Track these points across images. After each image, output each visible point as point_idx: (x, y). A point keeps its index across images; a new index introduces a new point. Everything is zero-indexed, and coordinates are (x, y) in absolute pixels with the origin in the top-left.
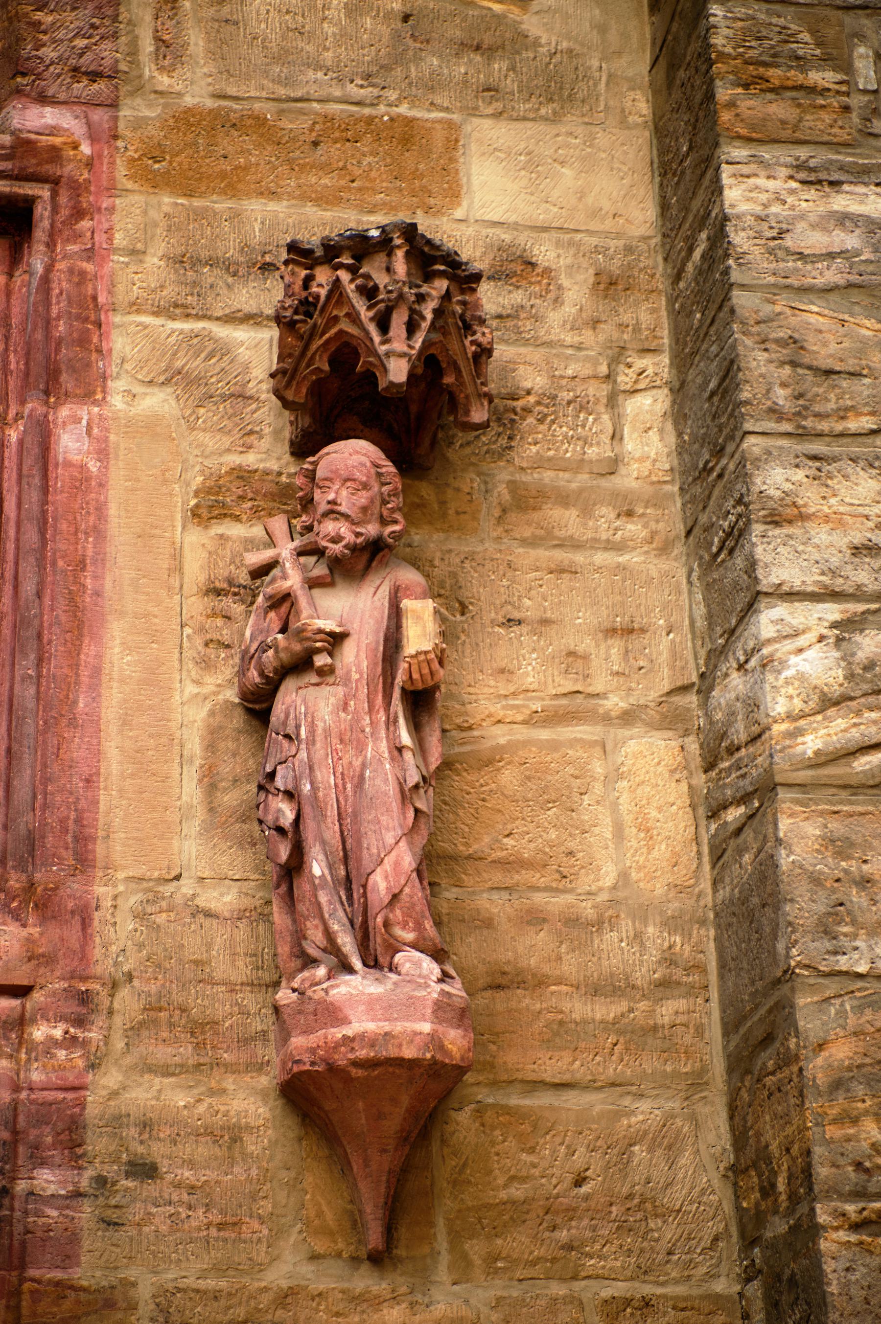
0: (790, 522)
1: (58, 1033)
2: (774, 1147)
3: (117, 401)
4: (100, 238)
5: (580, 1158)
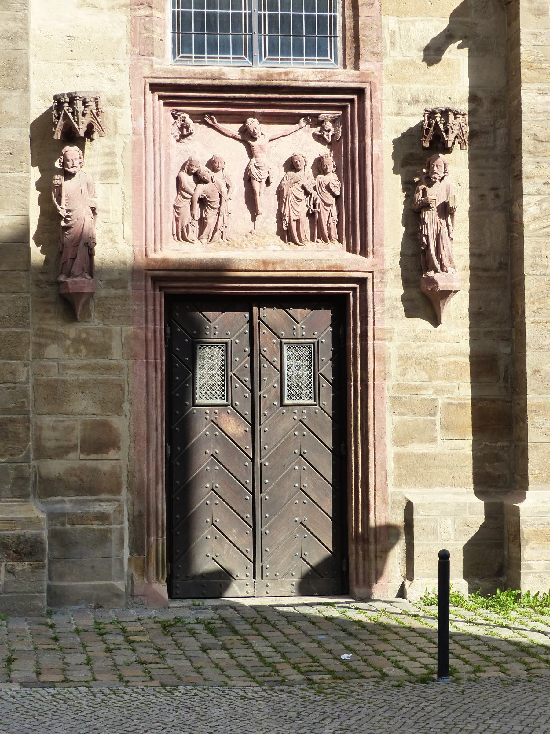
0: (531, 178)
4: (379, 96)
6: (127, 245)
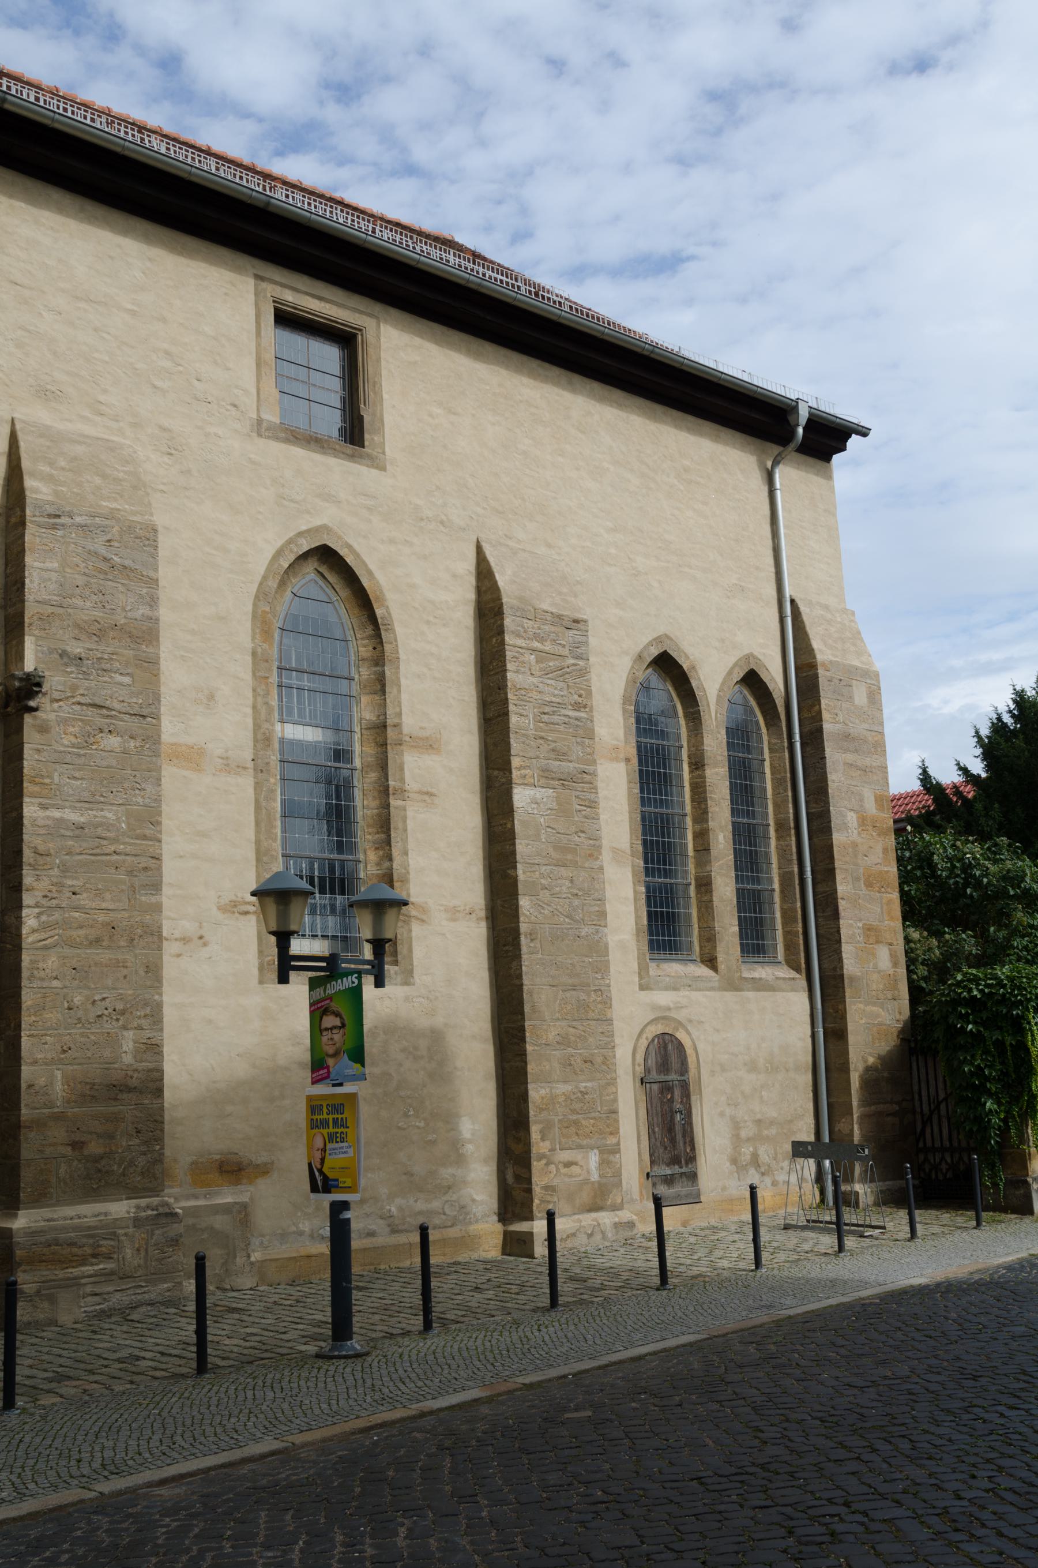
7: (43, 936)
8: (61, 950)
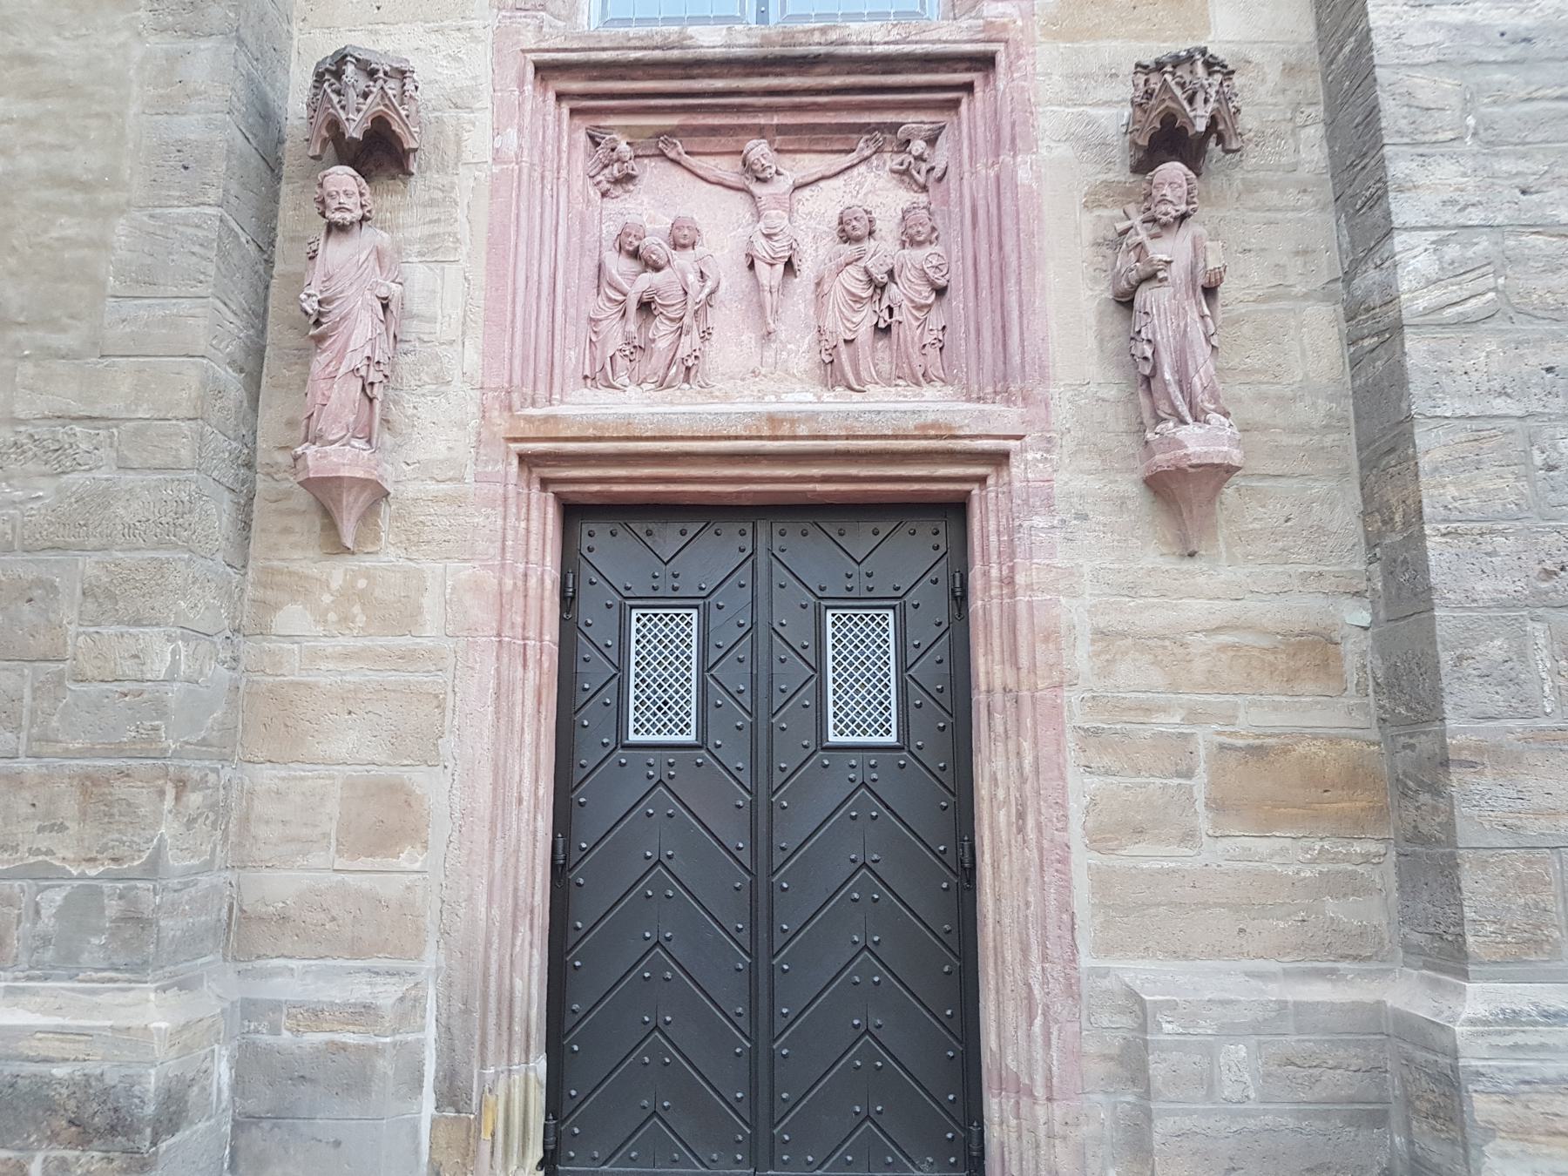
1: (1038, 456)
2: (1393, 501)
3: (1043, 151)
5: (1286, 511)
6: (467, 387)
7: (1453, 292)
8: (1508, 326)
